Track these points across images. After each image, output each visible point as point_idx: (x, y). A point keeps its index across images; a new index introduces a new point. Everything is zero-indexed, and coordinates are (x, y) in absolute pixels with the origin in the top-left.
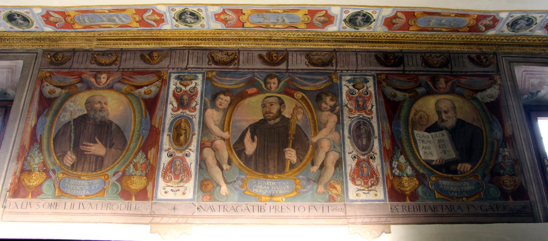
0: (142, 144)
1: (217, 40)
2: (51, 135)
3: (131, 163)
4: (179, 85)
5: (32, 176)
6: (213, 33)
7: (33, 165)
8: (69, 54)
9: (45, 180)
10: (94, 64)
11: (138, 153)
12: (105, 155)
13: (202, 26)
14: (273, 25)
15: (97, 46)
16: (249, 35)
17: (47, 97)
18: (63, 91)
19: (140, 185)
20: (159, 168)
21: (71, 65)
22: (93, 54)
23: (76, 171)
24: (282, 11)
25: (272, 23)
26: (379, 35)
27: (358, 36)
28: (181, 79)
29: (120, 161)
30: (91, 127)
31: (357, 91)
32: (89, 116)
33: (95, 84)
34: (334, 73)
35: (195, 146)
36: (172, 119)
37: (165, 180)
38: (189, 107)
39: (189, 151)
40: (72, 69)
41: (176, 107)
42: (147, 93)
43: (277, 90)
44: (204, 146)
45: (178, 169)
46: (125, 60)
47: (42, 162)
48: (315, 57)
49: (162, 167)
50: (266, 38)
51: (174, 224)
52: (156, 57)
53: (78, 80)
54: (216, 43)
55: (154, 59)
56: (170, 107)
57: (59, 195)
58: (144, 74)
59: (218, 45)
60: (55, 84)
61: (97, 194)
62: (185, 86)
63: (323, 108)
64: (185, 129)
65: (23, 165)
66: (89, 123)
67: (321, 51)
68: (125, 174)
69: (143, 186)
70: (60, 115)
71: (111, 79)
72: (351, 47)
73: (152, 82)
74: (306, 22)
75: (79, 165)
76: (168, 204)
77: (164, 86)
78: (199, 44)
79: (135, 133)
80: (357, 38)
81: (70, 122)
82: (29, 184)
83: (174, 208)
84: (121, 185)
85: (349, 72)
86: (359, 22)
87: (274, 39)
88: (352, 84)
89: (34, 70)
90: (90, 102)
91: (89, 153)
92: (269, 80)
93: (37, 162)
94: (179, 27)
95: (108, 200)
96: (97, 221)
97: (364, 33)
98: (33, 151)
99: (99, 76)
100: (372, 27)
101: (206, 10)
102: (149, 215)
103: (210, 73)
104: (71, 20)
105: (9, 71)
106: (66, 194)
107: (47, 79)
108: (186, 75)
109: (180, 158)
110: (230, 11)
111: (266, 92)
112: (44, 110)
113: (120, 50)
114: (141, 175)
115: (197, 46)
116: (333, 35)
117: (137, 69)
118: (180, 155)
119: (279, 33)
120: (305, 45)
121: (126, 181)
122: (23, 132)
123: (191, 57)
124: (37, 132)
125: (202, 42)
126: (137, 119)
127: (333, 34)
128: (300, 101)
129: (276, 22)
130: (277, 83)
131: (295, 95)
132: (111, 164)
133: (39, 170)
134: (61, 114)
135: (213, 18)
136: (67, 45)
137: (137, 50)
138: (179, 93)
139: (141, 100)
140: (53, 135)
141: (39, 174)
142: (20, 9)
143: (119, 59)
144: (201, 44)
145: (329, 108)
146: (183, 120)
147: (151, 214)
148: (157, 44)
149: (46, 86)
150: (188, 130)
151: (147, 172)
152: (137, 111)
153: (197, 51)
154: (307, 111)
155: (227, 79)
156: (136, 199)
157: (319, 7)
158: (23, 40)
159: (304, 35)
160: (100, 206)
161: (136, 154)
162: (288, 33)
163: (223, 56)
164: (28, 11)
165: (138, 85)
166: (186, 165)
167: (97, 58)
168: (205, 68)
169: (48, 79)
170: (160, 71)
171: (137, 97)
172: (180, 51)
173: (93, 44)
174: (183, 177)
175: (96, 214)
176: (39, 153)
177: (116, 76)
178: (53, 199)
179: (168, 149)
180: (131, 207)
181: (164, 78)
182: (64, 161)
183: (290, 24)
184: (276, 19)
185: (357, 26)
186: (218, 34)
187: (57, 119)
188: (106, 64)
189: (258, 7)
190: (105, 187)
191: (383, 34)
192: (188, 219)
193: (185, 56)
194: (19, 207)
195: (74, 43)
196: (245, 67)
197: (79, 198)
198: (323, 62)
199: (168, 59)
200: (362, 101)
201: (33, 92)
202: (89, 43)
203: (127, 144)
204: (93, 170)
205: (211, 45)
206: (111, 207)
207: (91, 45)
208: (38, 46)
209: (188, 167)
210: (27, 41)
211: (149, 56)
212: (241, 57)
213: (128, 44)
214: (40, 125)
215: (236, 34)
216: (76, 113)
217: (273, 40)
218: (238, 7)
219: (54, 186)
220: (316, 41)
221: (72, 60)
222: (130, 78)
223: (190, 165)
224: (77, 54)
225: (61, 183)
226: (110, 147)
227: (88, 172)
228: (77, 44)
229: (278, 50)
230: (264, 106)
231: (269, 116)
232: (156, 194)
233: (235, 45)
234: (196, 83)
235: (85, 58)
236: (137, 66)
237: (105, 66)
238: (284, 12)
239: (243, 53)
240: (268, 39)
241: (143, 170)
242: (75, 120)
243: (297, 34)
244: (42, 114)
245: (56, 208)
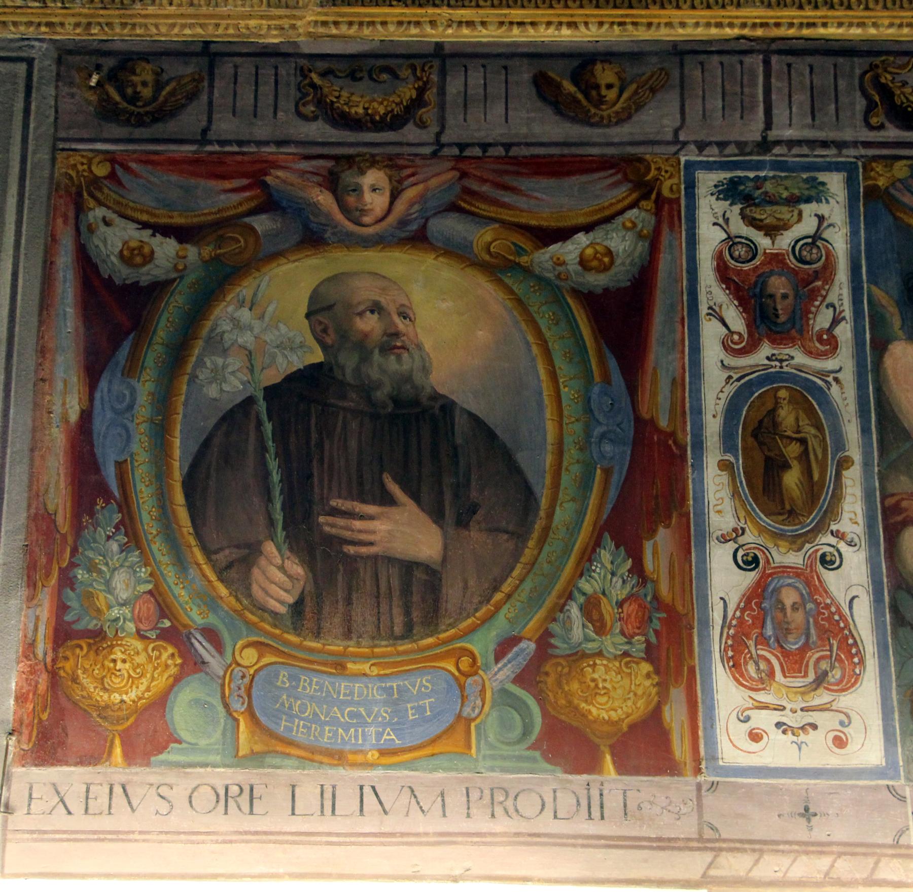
0: (609, 507)
2: (169, 467)
3: (570, 597)
4: (739, 227)
5: (114, 661)
7: (110, 607)
8: (190, 70)
9: (177, 679)
10: (315, 118)
11: (594, 550)
12: (444, 560)
15: (321, 30)
17: (117, 282)
18: (192, 252)
19: (630, 703)
20: (705, 623)
21: (204, 123)
22: (303, 72)
23: (317, 634)
28: (748, 200)
29: (517, 587)
30: (354, 425)
32: (338, 374)
33: (339, 217)
35: (860, 519)
36: (731, 389)
37: (742, 675)
38: (801, 332)
39: (833, 540)
40: (210, 143)
41: (740, 334)
42: (595, 263)
44: (899, 518)
45: (793, 626)
46: (460, 100)
47: (150, 592)
49: (717, 616)
51: (818, 884)
52: (609, 86)
53: (250, 199)
54: (898, 21)
55: (601, 100)
56: (711, 332)
57: (258, 748)
58: (569, 173)
60: (145, 218)
61: (434, 741)
62: (772, 231)
64: (797, 440)
65: (61, 608)
66: (344, 409)
68: (550, 651)
69: (641, 703)
70: (195, 367)
71: (410, 193)
73: (607, 213)
75: (326, 609)
76: (774, 790)
77: (671, 226)
78: (814, 25)
79: (566, 456)
81: (249, 401)
82: (106, 696)
83: (807, 809)
84: (542, 701)
89: (31, 148)
90: (330, 307)
91: (364, 550)
93: (124, 595)
95: (492, 769)
96: (457, 872)
98: (95, 541)
99: (348, 177)
102: (695, 844)
103: (879, 168)
106: (291, 743)
107: (100, 189)
108: (765, 178)
109: (798, 575)
112: (116, 345)
113: (431, 50)
114: (626, 654)
115: (806, 32)
117: (528, 145)
118: (795, 559)
121: (559, 684)
122: (32, 450)
123: (779, 90)
124: (98, 451)
125: (830, 13)
126: (564, 391)
132: (476, 600)
133: (138, 631)
134: (200, 363)
137: (513, 55)
138: (746, 267)
139: (570, 300)
140: (176, 464)
141: (146, 650)
143: (431, 95)
144: (825, 25)
146: (783, 394)
147: (700, 839)
148: (612, 23)
149: (103, 228)
150: (813, 443)
151: (653, 639)
152: (557, 348)
153: (809, 59)
156: (623, 768)
160: (456, 800)
161: (589, 555)
165: (544, 224)
166: (827, 607)
167: (326, 90)
168: (855, 144)
169: (106, 191)
170: (640, 160)
171: (548, 282)
172: (726, 59)
173: (299, 23)
174: (824, 665)
175: (446, 838)
176: (124, 548)
177: (434, 182)
178: (230, 771)
179: (735, 530)
180: (602, 807)
181: (666, 193)
182: (255, 589)
187: (185, 387)
188: (373, 121)
190: (467, 711)
192: (877, 863)
193: (754, 84)
194: (76, 806)
195: (211, 16)
197: (354, 765)
199: (671, 100)
201: (45, 262)
202: (280, 17)
203: (538, 508)
204: (398, 630)
205: (873, 31)
206: (509, 803)
207: (293, 27)
208: (30, 24)
209: (839, 611)
211: (576, 83)
213: (470, 24)
214: (109, 415)
216: (273, 357)
219: (226, 706)
221: (204, 98)
222: (502, 192)
223: (851, 608)
224: (226, 68)
225: (254, 692)
226: (462, 523)
227: (373, 638)
228: (222, 17)
232: (712, 743)
234: (821, 218)
235: (267, 89)
236: (524, 130)
237: (369, 130)
241: (629, 629)
242: (271, 392)
244: (108, 360)
245: (251, 813)
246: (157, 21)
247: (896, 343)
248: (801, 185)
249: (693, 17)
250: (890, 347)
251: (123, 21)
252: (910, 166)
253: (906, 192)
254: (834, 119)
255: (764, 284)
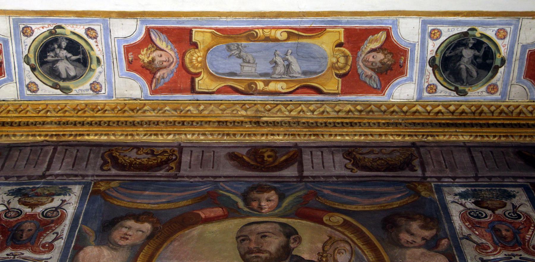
1: (128, 124)
6: (119, 108)
13: (95, 88)
14: (263, 81)
16: (206, 113)
24: (285, 36)
25: (261, 75)
26: (518, 110)
27: (466, 113)
31: (489, 212)
34: (419, 183)
38: (33, 244)
43: (276, 211)
48: (366, 156)
50: (247, 120)
54: (125, 133)
59: (129, 137)
63: (402, 241)
67: (382, 146)
72: (453, 138)
74: (341, 69)
78: (83, 135)
80: (464, 116)
85: (457, 180)
86: (467, 69)
87: (267, 122)
88: (473, 201)
92: (255, 195)
94: (39, 93)
97: (481, 105)
100: (499, 84)
101: (107, 31)
110: (163, 36)
111: (248, 215)
115: (78, 138)
116: (407, 112)
119: (278, 107)
120: (340, 135)
127: (405, 109)
128: (339, 229)
129: (270, 71)
130: (277, 200)
131: (325, 219)
135: (121, 59)
144: (88, 135)
145: (419, 241)
154: (361, 247)
155: (147, 193)
157: (369, 18)
159: (338, 112)
162: (300, 108)
163: (139, 156)
183: (303, 77)
184: (271, 62)
185: (462, 83)
186: (132, 110)
189: (229, 19)
191: (527, 106)
193: (45, 156)
196: (195, 174)
198: (387, 163)
200: (507, 230)
205: (113, 138)
212: (186, 158)
215: (175, 110)
217: (263, 123)
218: (183, 22)
220: (367, 125)
229: (275, 145)
230: (243, 240)
231: (257, 257)
233: (171, 137)
238: (288, 39)
239: (192, 151)
240: (251, 122)
243: (321, 110)
247: (89, 247)
248: (58, 190)
249: (20, 132)
250: (85, 248)
252: (119, 183)
253: (114, 191)
254: (85, 167)
255: (21, 225)
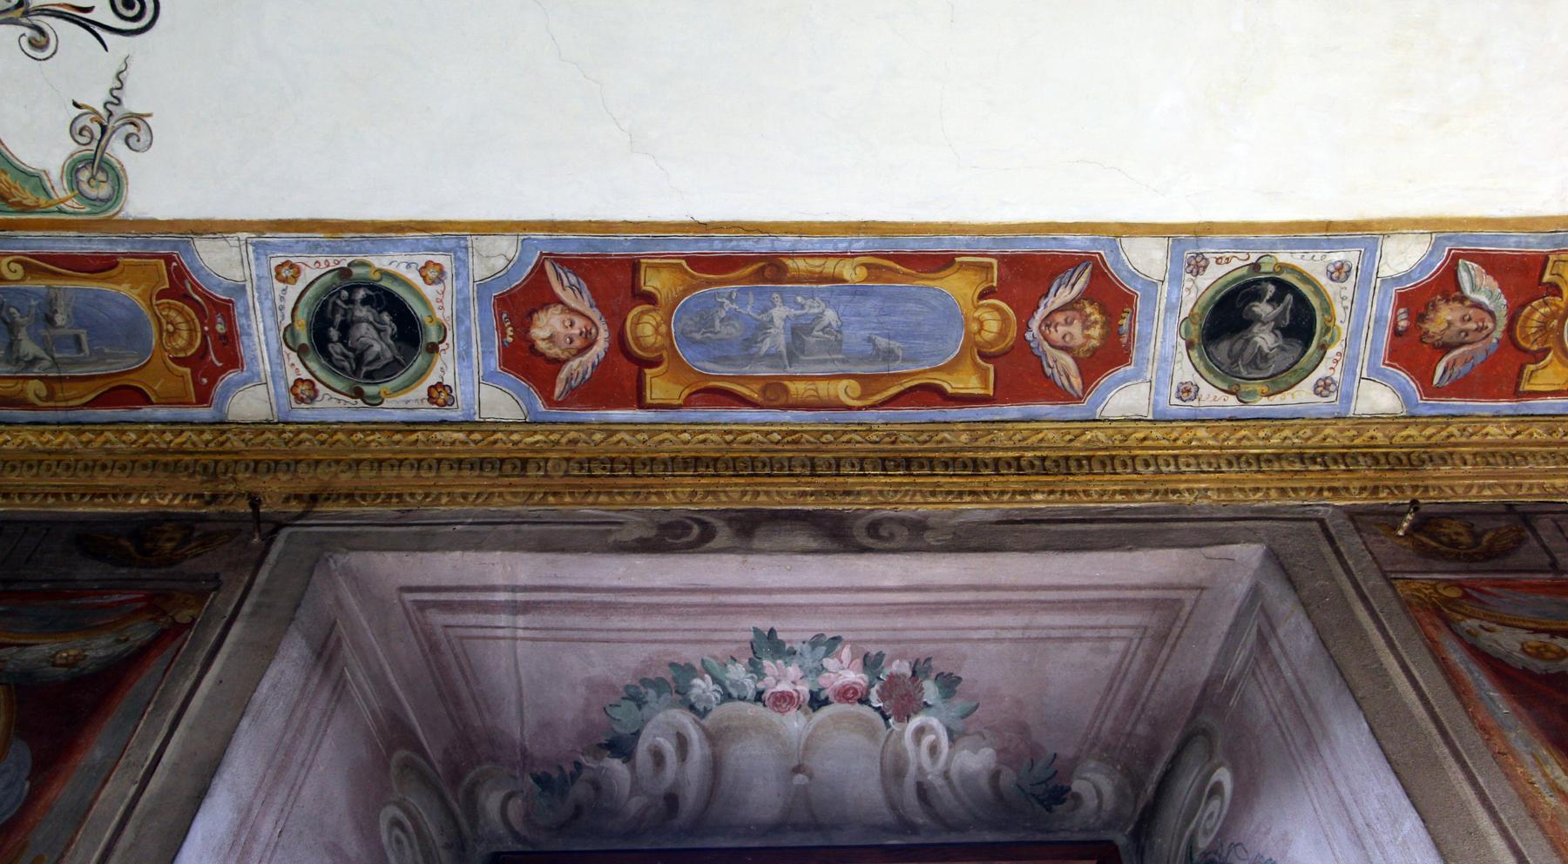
8: (1503, 524)
60: (1531, 625)
104: (1543, 327)
105: (1146, 628)
107: (1461, 606)
136: (1470, 487)
142: (1315, 245)
158: (1230, 464)
164: (1351, 256)
210: (1255, 468)
246: (1452, 482)
251: (1414, 483)
